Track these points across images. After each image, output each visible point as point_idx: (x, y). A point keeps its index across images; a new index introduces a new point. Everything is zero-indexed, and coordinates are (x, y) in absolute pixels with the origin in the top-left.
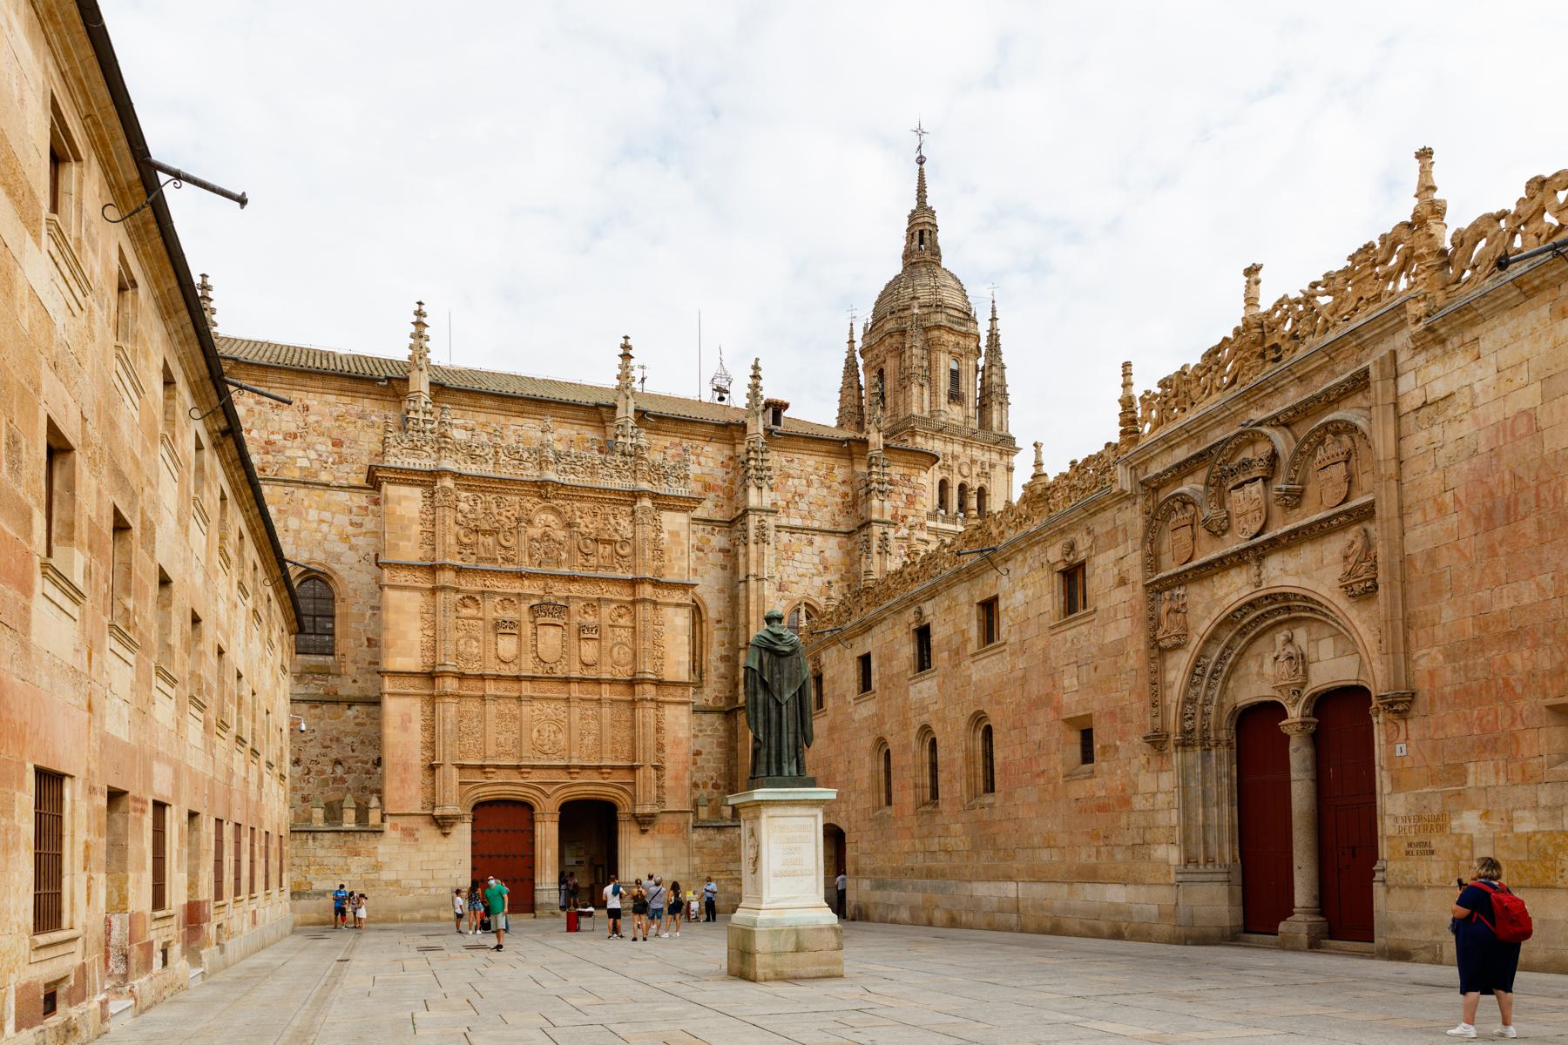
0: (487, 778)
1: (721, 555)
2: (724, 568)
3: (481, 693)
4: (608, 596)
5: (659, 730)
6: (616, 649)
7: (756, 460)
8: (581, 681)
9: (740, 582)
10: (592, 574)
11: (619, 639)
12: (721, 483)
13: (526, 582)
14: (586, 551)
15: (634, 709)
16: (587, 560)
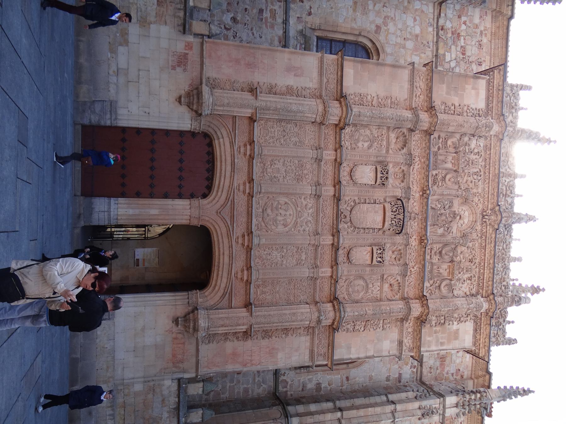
1: (397, 376)
2: (388, 379)
4: (409, 274)
5: (286, 331)
6: (361, 282)
7: (475, 400)
8: (335, 248)
9: (387, 397)
10: (428, 257)
11: (371, 286)
12: (446, 371)
13: (417, 195)
14: (443, 252)
15: (307, 304)
16: (435, 253)
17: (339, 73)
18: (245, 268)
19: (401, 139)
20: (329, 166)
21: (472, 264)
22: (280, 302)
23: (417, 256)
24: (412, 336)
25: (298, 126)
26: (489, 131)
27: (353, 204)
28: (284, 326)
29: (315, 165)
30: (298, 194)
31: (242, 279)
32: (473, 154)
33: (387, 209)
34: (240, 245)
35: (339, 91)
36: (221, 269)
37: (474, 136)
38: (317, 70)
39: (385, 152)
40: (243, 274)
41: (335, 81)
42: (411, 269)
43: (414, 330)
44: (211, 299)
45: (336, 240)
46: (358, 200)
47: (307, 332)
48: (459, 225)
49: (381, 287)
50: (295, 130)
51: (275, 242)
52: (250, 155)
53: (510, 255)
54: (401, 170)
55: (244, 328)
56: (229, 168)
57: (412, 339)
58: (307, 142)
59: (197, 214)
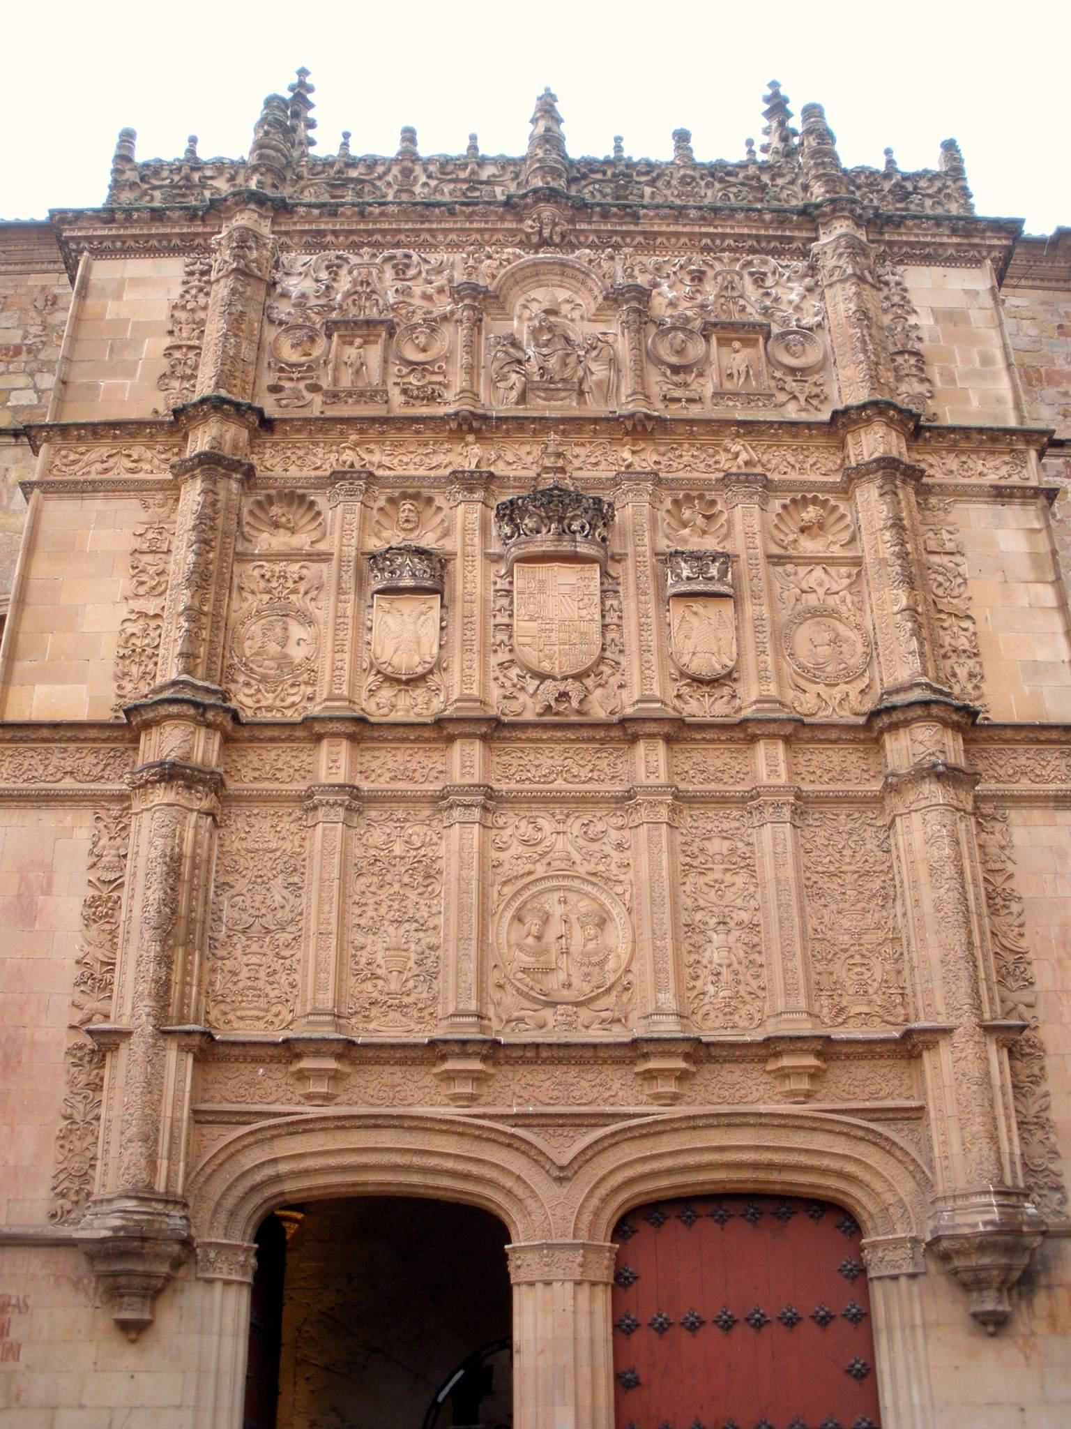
0: (309, 1097)
3: (302, 786)
4: (759, 470)
10: (695, 411)
11: (812, 600)
13: (476, 450)
14: (674, 360)
15: (892, 825)
17: (45, 733)
18: (771, 1066)
19: (280, 512)
20: (378, 762)
21: (710, 273)
22: (890, 924)
23: (692, 445)
24: (974, 457)
25: (229, 879)
26: (257, 237)
27: (514, 672)
28: (978, 906)
29: (373, 814)
30: (482, 871)
31: (815, 1075)
32: (335, 285)
33: (533, 549)
34: (685, 1090)
35: (107, 734)
36: (777, 1158)
37: (275, 284)
38: (32, 812)
39: (323, 566)
40: (797, 1072)
41: (72, 747)
42: (740, 461)
43: (953, 449)
44: (891, 1188)
45: (651, 728)
46: (500, 654)
47: (993, 823)
48: (576, 314)
49: (812, 561)
50: (244, 891)
51: (670, 952)
52: (339, 1057)
53: (672, 163)
54: (388, 507)
55: (996, 1057)
56: (386, 1139)
57: (983, 454)
58: (287, 845)
59: (568, 1254)
